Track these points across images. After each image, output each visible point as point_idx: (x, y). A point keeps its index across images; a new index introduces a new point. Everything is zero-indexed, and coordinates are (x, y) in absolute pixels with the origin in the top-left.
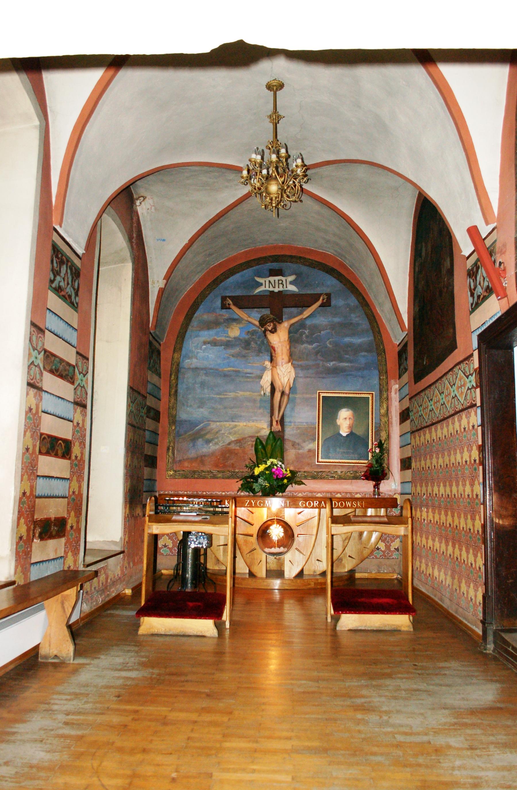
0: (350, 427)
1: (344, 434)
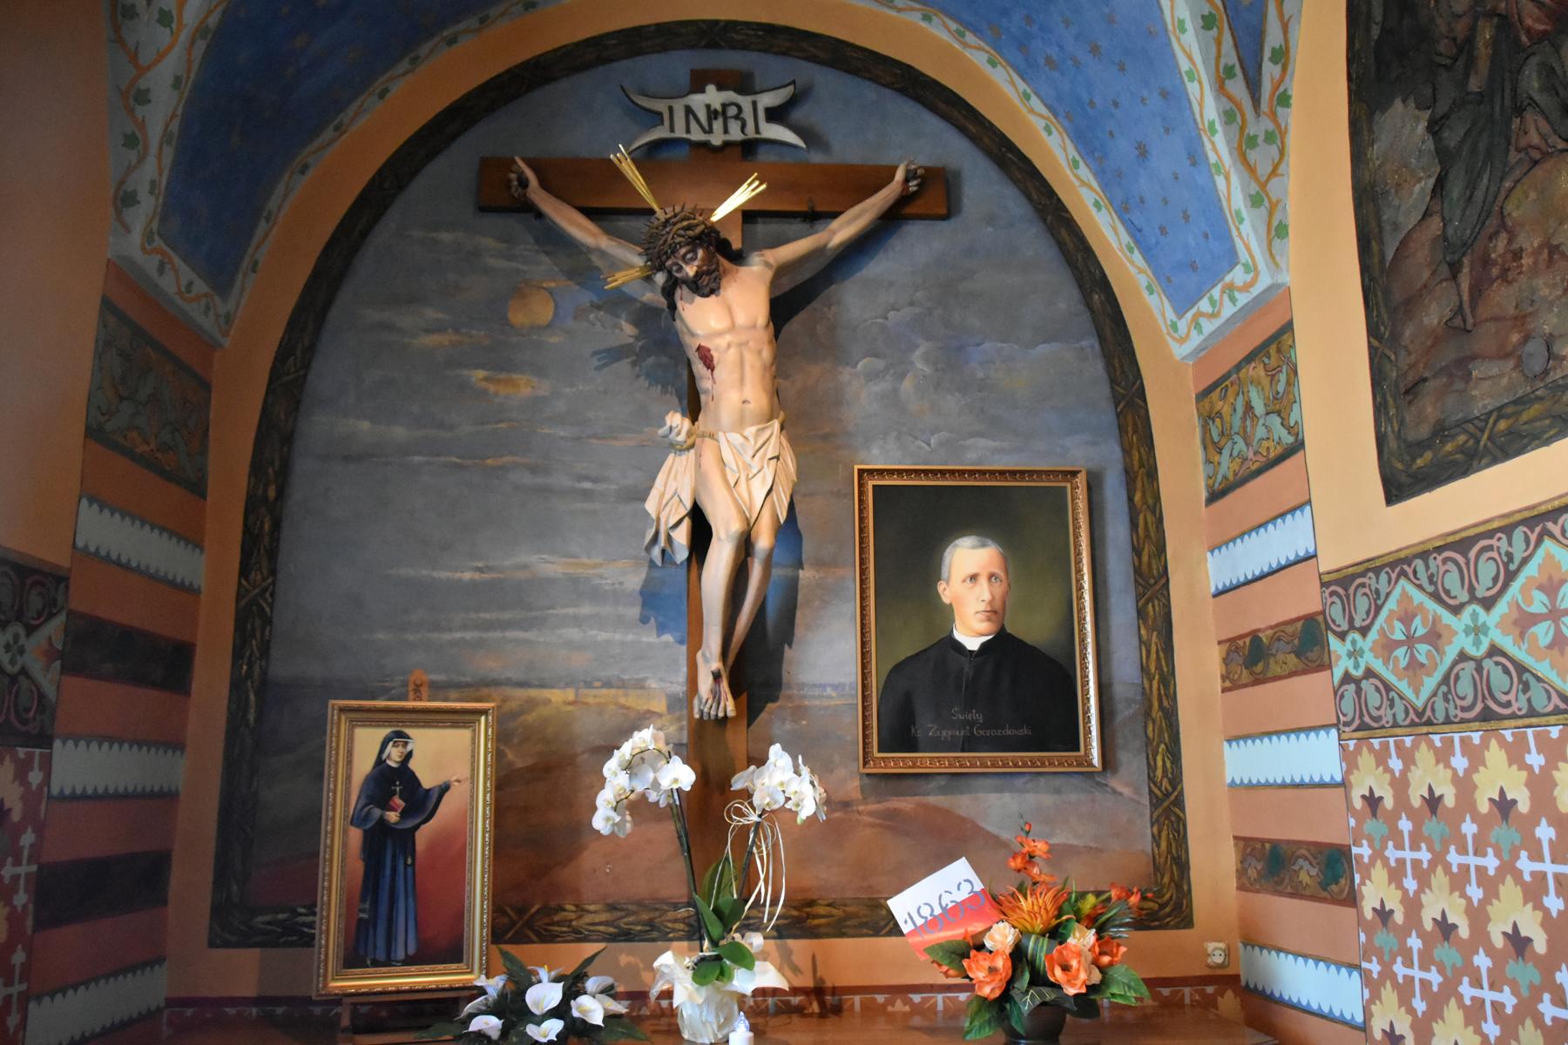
0: (994, 613)
1: (973, 644)
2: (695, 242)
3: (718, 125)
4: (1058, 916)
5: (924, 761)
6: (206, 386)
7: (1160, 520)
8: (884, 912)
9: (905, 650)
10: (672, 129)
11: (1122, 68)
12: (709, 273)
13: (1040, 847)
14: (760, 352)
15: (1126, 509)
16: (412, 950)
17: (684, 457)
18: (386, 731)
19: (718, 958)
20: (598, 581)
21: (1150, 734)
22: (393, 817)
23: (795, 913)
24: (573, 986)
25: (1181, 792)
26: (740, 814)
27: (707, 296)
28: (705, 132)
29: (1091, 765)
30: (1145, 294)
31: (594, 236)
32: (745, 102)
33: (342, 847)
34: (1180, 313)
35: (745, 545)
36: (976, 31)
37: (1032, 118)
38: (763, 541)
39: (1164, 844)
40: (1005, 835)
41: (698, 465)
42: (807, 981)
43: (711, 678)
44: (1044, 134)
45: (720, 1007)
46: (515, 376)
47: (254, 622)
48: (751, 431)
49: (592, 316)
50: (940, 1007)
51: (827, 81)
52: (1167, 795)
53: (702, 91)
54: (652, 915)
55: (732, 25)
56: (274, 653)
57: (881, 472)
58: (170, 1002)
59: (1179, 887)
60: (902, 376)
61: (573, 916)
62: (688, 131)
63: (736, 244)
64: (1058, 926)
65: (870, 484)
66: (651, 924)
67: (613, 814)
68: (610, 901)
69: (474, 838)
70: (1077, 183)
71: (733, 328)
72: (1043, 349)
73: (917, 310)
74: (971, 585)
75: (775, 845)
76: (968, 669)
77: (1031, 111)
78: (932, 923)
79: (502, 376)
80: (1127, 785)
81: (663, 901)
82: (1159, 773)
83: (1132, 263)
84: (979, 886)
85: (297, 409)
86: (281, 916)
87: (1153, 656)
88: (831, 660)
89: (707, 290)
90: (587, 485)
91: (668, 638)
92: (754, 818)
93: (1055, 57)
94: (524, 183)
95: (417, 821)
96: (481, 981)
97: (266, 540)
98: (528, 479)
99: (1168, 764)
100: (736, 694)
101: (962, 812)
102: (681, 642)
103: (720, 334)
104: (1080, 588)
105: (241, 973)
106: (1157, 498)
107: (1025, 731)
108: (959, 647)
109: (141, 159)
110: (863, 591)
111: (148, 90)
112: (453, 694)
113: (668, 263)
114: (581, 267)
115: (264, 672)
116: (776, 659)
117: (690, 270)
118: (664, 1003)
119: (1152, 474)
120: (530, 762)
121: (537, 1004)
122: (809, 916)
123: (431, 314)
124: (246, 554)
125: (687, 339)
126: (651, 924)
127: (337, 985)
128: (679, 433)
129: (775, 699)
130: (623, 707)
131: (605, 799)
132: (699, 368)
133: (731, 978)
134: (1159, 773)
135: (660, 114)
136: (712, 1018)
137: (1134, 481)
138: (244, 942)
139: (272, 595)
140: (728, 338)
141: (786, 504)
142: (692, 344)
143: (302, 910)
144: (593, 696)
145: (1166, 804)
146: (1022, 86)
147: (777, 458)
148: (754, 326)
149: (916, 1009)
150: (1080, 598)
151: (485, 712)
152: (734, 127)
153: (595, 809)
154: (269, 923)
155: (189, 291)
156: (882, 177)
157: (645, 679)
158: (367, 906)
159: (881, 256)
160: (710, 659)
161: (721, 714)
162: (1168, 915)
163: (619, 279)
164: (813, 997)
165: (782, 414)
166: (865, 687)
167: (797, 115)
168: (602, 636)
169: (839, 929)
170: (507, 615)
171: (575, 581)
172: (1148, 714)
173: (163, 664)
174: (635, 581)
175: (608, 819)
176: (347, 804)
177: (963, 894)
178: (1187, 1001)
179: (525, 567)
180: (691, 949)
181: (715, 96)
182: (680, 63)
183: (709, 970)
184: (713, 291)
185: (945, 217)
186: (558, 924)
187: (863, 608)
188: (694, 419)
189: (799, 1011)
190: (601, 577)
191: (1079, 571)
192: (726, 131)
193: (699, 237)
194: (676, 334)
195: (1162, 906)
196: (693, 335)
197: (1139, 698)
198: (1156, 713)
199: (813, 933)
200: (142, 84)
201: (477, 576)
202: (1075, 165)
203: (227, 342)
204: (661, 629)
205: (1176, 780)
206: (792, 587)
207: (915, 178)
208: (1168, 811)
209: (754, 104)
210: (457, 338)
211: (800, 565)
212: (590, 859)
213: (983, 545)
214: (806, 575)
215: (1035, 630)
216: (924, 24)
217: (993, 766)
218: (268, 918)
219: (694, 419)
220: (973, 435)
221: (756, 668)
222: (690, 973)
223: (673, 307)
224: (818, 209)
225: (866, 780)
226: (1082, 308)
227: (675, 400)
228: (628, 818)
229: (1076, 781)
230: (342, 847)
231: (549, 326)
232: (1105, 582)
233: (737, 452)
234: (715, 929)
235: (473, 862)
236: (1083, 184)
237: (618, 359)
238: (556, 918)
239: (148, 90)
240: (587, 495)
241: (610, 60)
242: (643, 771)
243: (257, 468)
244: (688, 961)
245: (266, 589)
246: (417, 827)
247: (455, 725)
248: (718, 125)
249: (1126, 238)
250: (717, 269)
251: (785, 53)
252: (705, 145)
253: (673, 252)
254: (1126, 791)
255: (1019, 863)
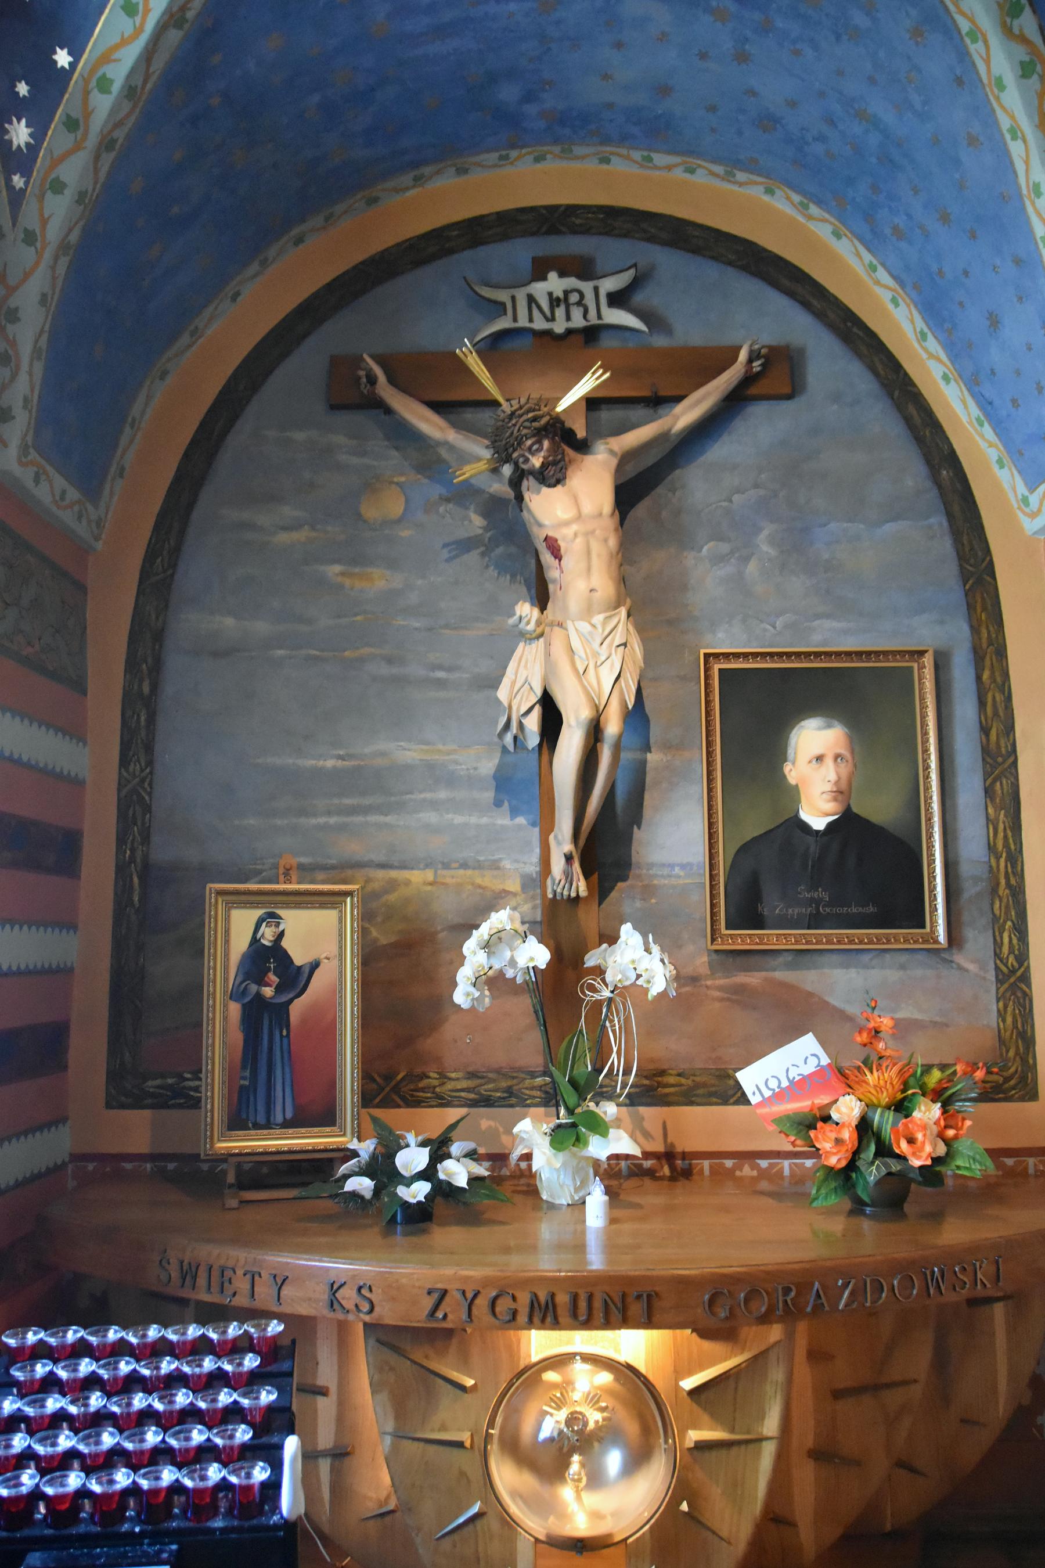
0: (840, 793)
1: (819, 823)
2: (540, 433)
3: (560, 312)
4: (904, 1091)
5: (771, 937)
6: (81, 588)
7: (1009, 698)
8: (731, 1082)
9: (752, 829)
10: (515, 320)
11: (973, 236)
12: (555, 463)
13: (886, 1023)
14: (606, 540)
15: (973, 687)
16: (289, 1115)
17: (534, 645)
18: (260, 912)
19: (574, 1125)
20: (451, 767)
21: (997, 912)
22: (268, 992)
23: (647, 1082)
24: (439, 1151)
25: (1028, 967)
26: (593, 989)
27: (554, 486)
28: (547, 320)
29: (936, 942)
30: (995, 468)
31: (441, 429)
32: (587, 287)
33: (223, 1022)
34: (1032, 489)
35: (595, 731)
36: (819, 203)
37: (878, 290)
38: (612, 727)
39: (1009, 1020)
40: (854, 1009)
41: (548, 654)
42: (659, 1147)
43: (563, 860)
44: (890, 306)
45: (577, 1171)
46: (369, 570)
47: (135, 809)
48: (598, 619)
49: (441, 509)
50: (787, 1172)
51: (667, 261)
52: (1013, 972)
53: (544, 278)
54: (509, 1083)
55: (572, 210)
56: (155, 839)
57: (726, 656)
58: (75, 1157)
59: (1024, 1061)
60: (746, 559)
61: (436, 1083)
62: (531, 320)
63: (581, 433)
64: (904, 1099)
65: (717, 667)
66: (510, 1091)
67: (472, 989)
68: (470, 1069)
69: (343, 1011)
70: (925, 356)
71: (579, 517)
72: (889, 528)
73: (762, 492)
74: (817, 767)
75: (627, 1019)
76: (814, 849)
77: (877, 282)
78: (779, 1096)
79: (357, 570)
80: (974, 961)
81: (520, 1070)
82: (1005, 949)
83: (982, 436)
84: (825, 1060)
85: (167, 606)
86: (170, 1081)
87: (1001, 835)
88: (678, 840)
89: (553, 481)
90: (441, 674)
91: (521, 820)
92: (606, 993)
93: (902, 225)
94: (372, 380)
95: (291, 995)
96: (354, 1145)
97: (143, 733)
98: (385, 670)
99: (1015, 941)
100: (587, 875)
101: (809, 988)
102: (534, 825)
103: (567, 523)
104: (927, 768)
105: (136, 1131)
106: (1006, 675)
107: (871, 909)
108: (805, 827)
109: (14, 376)
110: (710, 773)
111: (17, 309)
112: (321, 876)
113: (515, 455)
114: (429, 460)
115: (146, 857)
116: (627, 840)
117: (536, 462)
118: (523, 1165)
119: (1001, 652)
120: (393, 939)
121: (406, 1167)
122: (660, 1085)
123: (288, 512)
124: (126, 747)
125: (535, 530)
126: (510, 1091)
127: (223, 1146)
128: (528, 623)
129: (624, 878)
130: (480, 887)
131: (465, 975)
132: (547, 558)
133: (586, 1144)
134: (1005, 949)
135: (503, 305)
136: (569, 1182)
137: (983, 659)
138: (137, 1103)
139: (150, 785)
140: (575, 527)
141: (634, 689)
142: (539, 535)
143: (189, 1076)
144: (453, 876)
145: (1012, 980)
146: (867, 257)
147: (625, 645)
148: (600, 515)
149: (763, 1174)
150: (927, 777)
151: (349, 894)
152: (577, 313)
153: (454, 985)
154: (158, 1087)
155: (62, 498)
156: (725, 357)
157: (500, 859)
158: (247, 1073)
159: (725, 438)
160: (562, 841)
161: (573, 895)
162: (1013, 1088)
163: (468, 472)
164: (664, 1162)
165: (628, 601)
166: (712, 867)
167: (639, 298)
168: (459, 819)
169: (688, 1098)
170: (367, 801)
171: (431, 767)
172: (994, 891)
173: (54, 851)
174: (488, 766)
175: (468, 994)
176: (226, 980)
177: (810, 1068)
178: (1031, 1171)
179: (383, 754)
180: (547, 1115)
181: (555, 284)
182: (522, 251)
183: (566, 1136)
184: (559, 482)
185: (789, 397)
186: (423, 1090)
187: (710, 790)
188: (543, 608)
189: (650, 1173)
190: (456, 763)
191: (926, 751)
192: (568, 318)
193: (545, 428)
194: (524, 525)
195: (1007, 1080)
196: (540, 525)
197: (985, 876)
198: (1003, 891)
199: (664, 1101)
200: (12, 303)
201: (340, 763)
202: (923, 336)
203: (99, 546)
204: (514, 812)
205: (1023, 957)
206: (641, 769)
207: (758, 357)
208: (1013, 987)
209: (596, 290)
210: (314, 534)
211: (648, 748)
212: (451, 1030)
213: (829, 726)
214: (653, 758)
215: (881, 809)
216: (766, 198)
217: (839, 942)
218: (158, 1082)
219: (543, 608)
220: (818, 616)
221: (606, 848)
222: (548, 1139)
223: (520, 498)
224: (662, 393)
225: (714, 956)
226: (929, 484)
227: (524, 589)
228: (487, 993)
229: (920, 957)
230: (223, 1022)
231: (399, 521)
232: (952, 762)
233: (585, 640)
234: (571, 1098)
235: (343, 1034)
236: (931, 356)
237: (468, 551)
238: (421, 1085)
239: (17, 309)
240: (441, 684)
241: (451, 252)
242: (500, 951)
243: (132, 665)
244: (546, 1128)
245: (143, 781)
246: (291, 1001)
247: (323, 906)
248: (560, 312)
249: (975, 411)
250: (563, 459)
251: (626, 235)
252: (548, 333)
253: (520, 444)
254: (972, 967)
255: (865, 1037)
